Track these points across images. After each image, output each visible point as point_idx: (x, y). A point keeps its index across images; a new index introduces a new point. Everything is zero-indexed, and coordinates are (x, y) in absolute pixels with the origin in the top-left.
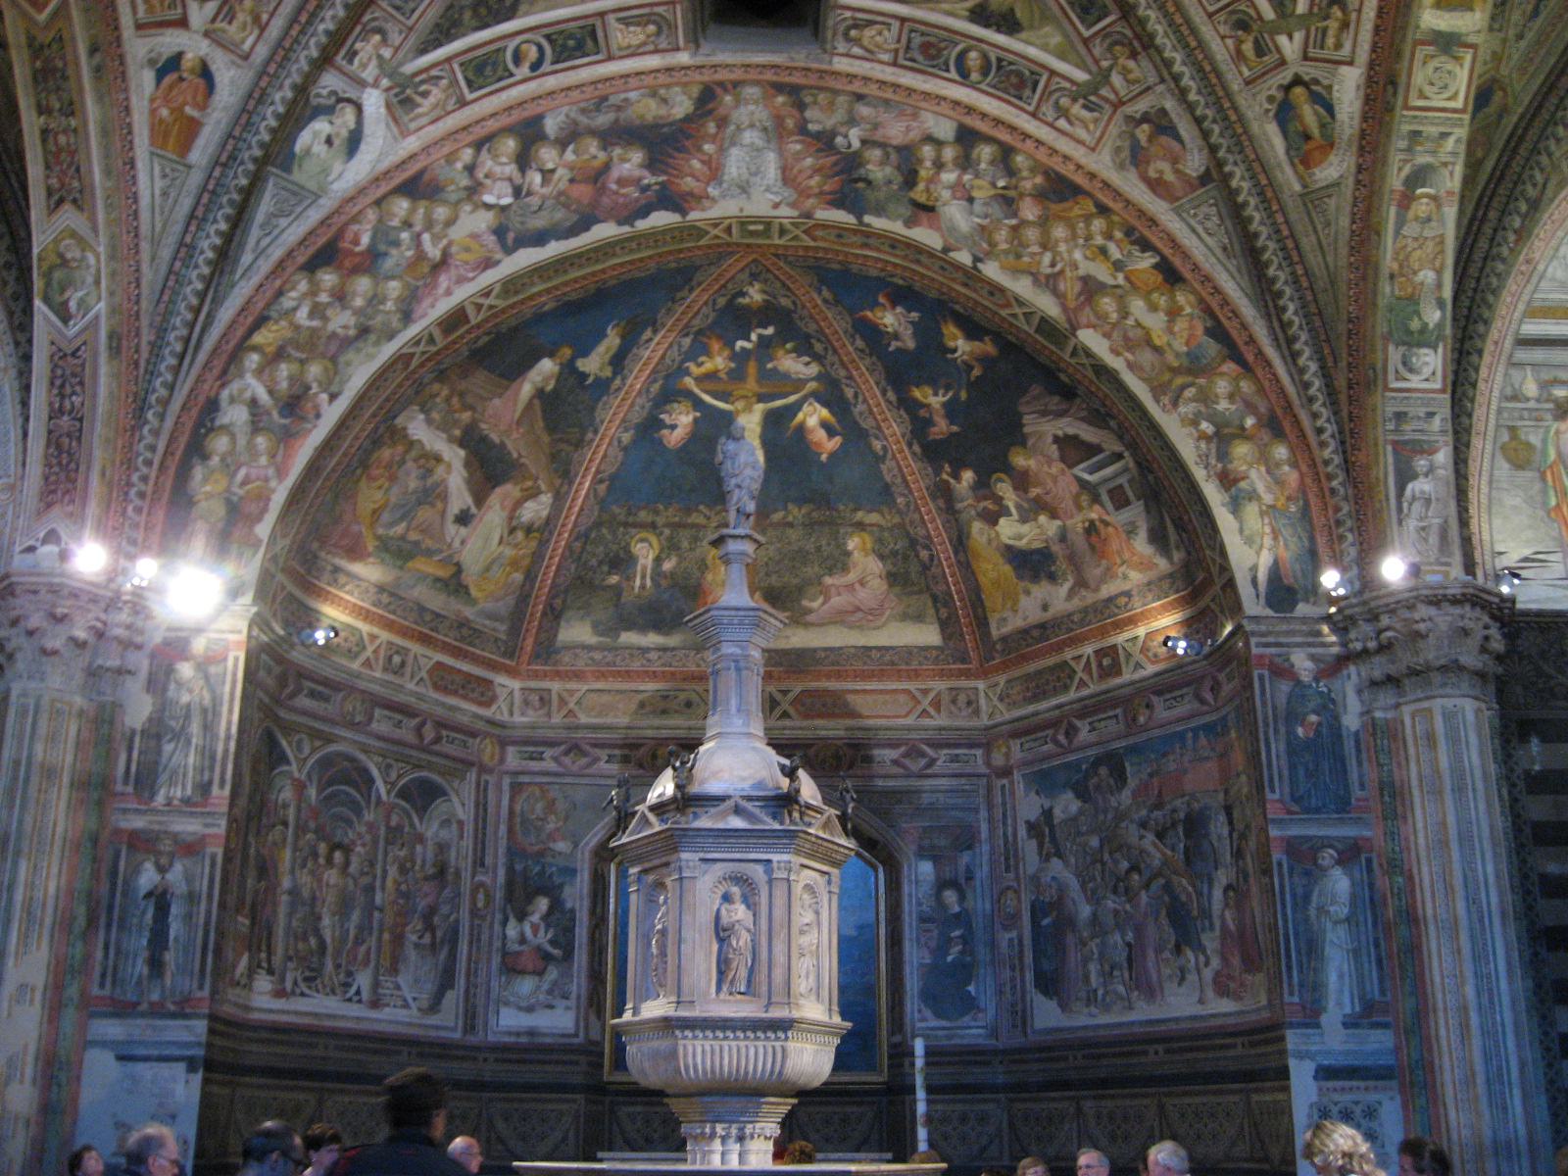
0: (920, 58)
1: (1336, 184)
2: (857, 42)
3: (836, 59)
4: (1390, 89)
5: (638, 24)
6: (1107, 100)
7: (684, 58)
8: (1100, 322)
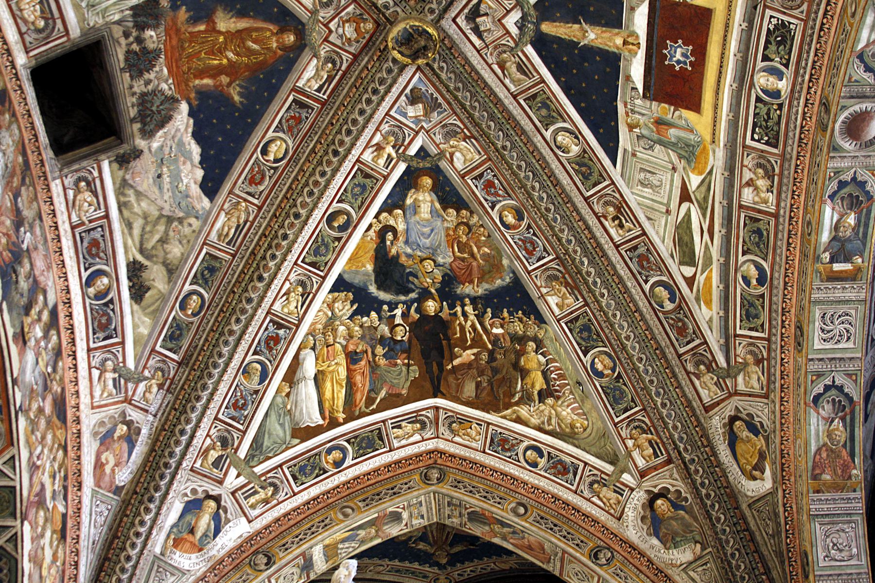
0: (85, 244)
1: (183, 573)
2: (78, 191)
3: (58, 181)
4: (262, 560)
5: (42, 11)
6: (126, 391)
7: (21, 59)
8: (33, 528)
